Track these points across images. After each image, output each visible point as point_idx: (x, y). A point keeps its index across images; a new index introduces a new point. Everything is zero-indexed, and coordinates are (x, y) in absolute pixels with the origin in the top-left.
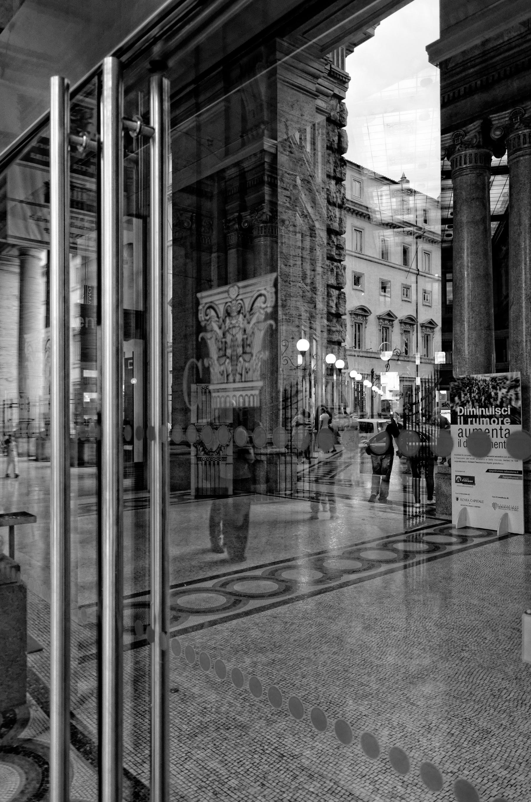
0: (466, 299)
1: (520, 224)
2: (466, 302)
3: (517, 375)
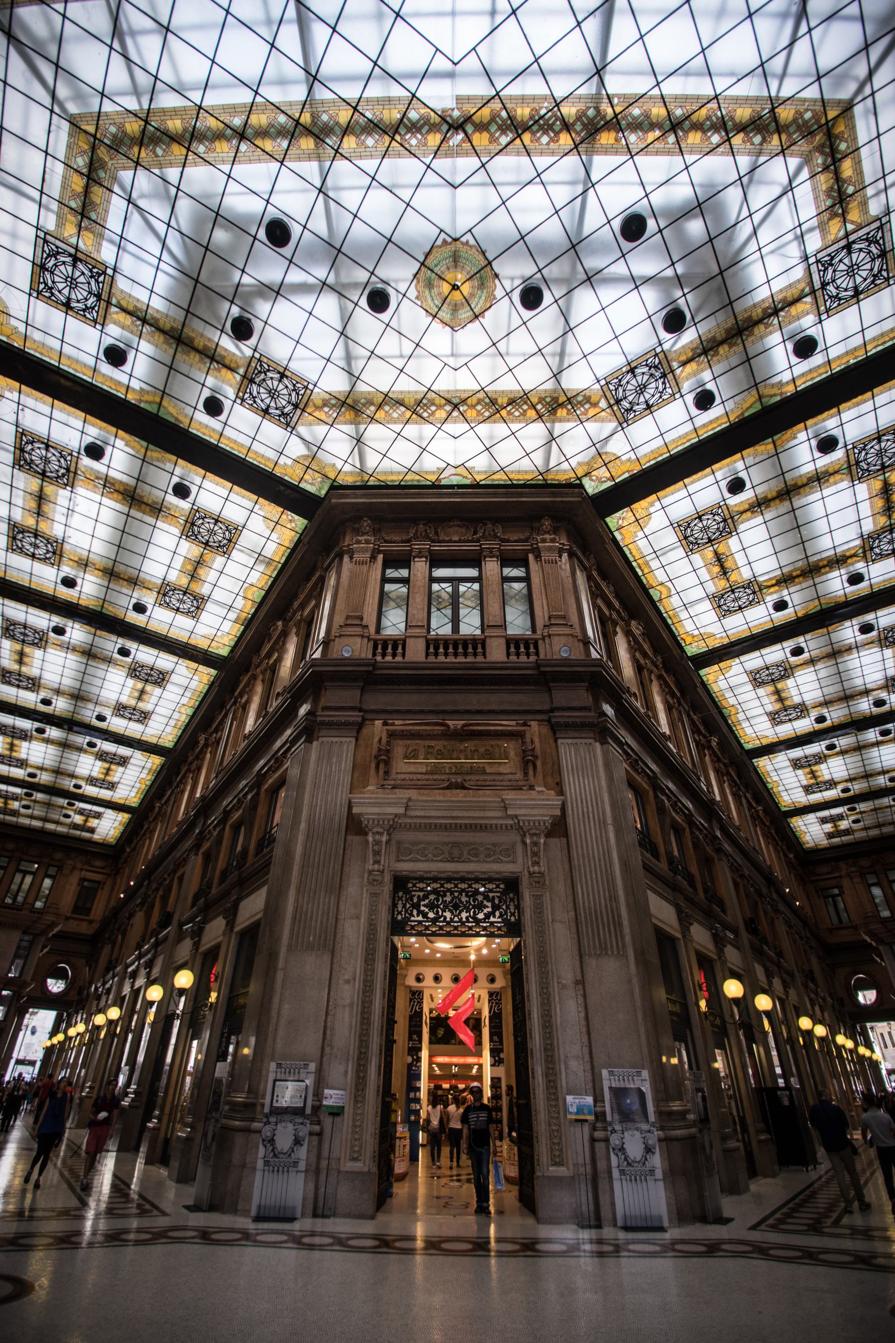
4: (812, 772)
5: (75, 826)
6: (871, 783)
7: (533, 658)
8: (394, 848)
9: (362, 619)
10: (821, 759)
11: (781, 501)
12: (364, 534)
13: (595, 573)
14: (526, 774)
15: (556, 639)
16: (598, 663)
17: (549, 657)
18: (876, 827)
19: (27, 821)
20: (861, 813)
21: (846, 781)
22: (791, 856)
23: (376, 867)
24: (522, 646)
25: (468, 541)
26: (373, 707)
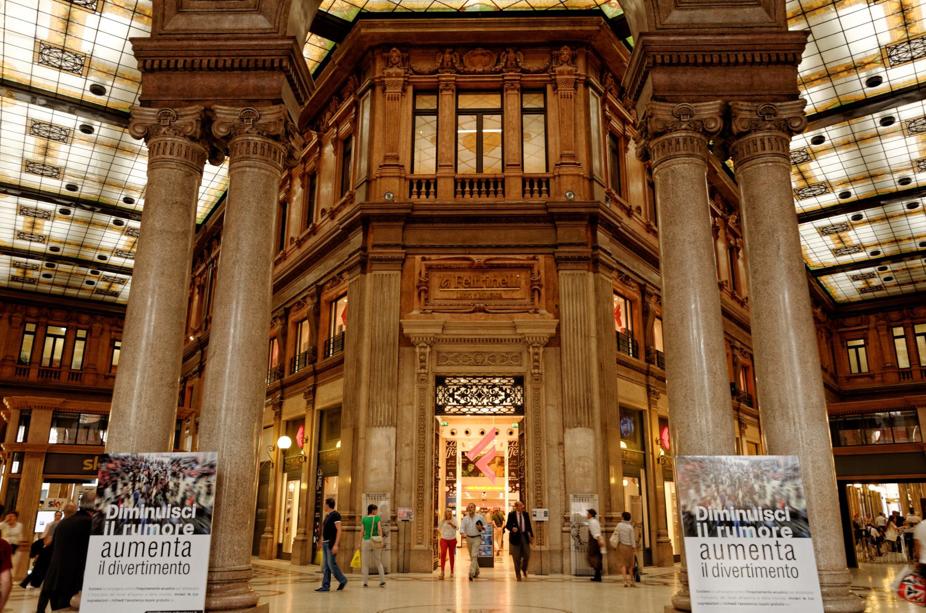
0: (145, 338)
1: (237, 249)
2: (144, 343)
3: (212, 456)
4: (840, 238)
5: (100, 291)
7: (545, 195)
8: (435, 357)
9: (398, 159)
11: (797, 20)
12: (394, 65)
13: (609, 96)
14: (533, 299)
15: (564, 179)
16: (597, 205)
17: (557, 199)
18: (909, 283)
19: (47, 288)
20: (894, 271)
21: (876, 245)
22: (818, 311)
23: (423, 371)
24: (536, 184)
25: (491, 73)
26: (414, 244)
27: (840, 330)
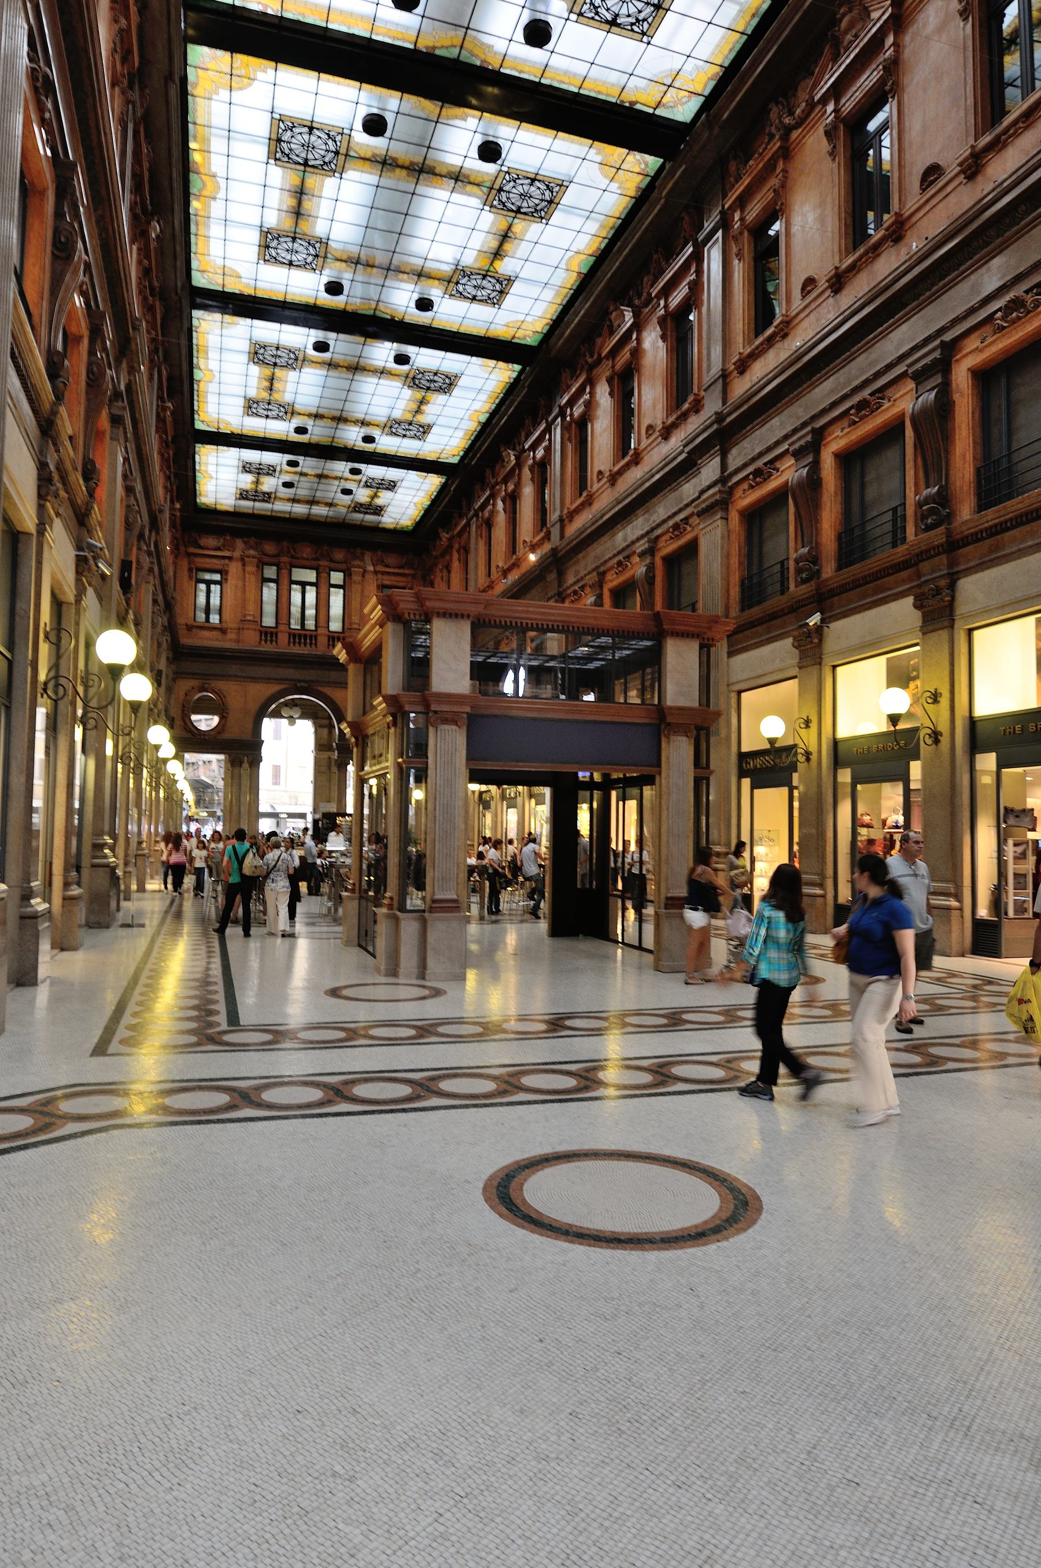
4: (272, 380)
6: (339, 434)
10: (296, 360)
20: (302, 474)
21: (310, 415)
27: (192, 550)
